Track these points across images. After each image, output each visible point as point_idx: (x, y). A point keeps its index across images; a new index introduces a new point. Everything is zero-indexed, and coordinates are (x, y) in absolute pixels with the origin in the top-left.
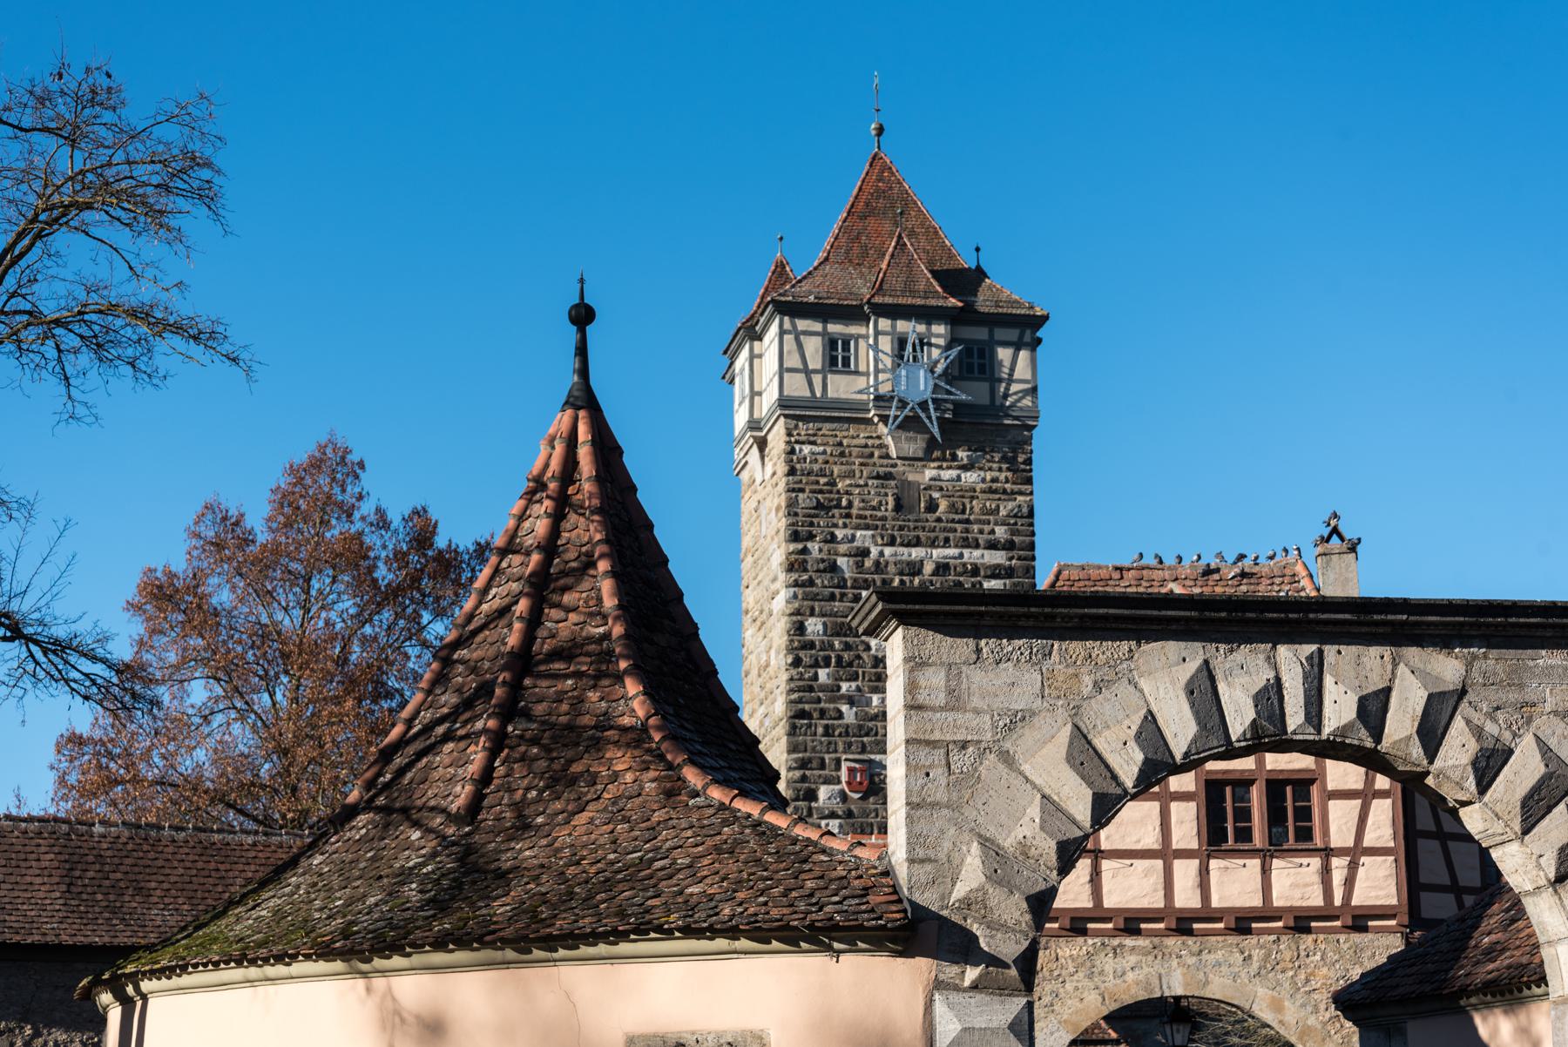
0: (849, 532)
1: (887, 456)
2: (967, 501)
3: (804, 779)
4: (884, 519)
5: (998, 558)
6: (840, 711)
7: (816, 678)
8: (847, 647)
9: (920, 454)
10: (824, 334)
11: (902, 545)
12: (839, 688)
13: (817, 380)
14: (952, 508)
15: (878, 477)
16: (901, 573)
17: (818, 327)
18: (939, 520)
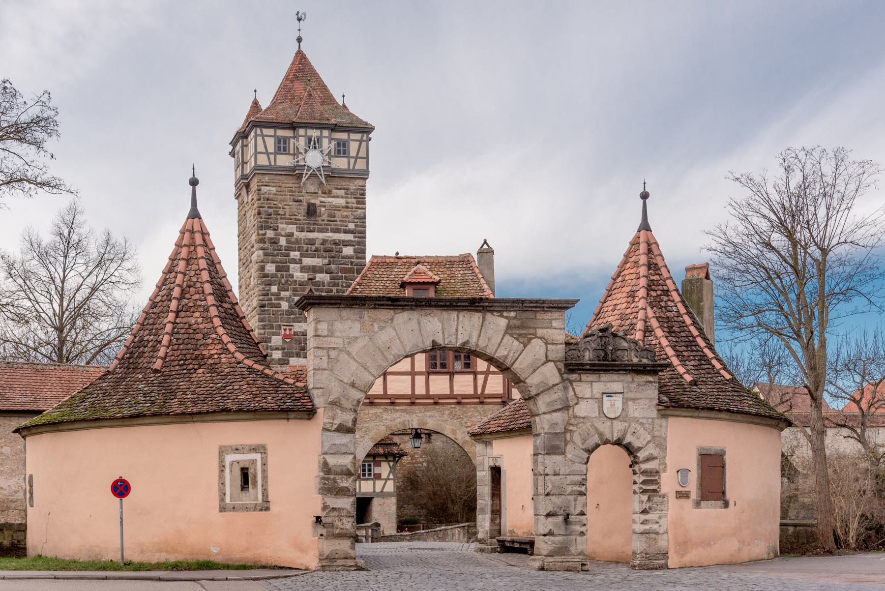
0: (285, 226)
5: (350, 237)
7: (270, 290)
10: (275, 136)
13: (272, 157)
14: (330, 215)
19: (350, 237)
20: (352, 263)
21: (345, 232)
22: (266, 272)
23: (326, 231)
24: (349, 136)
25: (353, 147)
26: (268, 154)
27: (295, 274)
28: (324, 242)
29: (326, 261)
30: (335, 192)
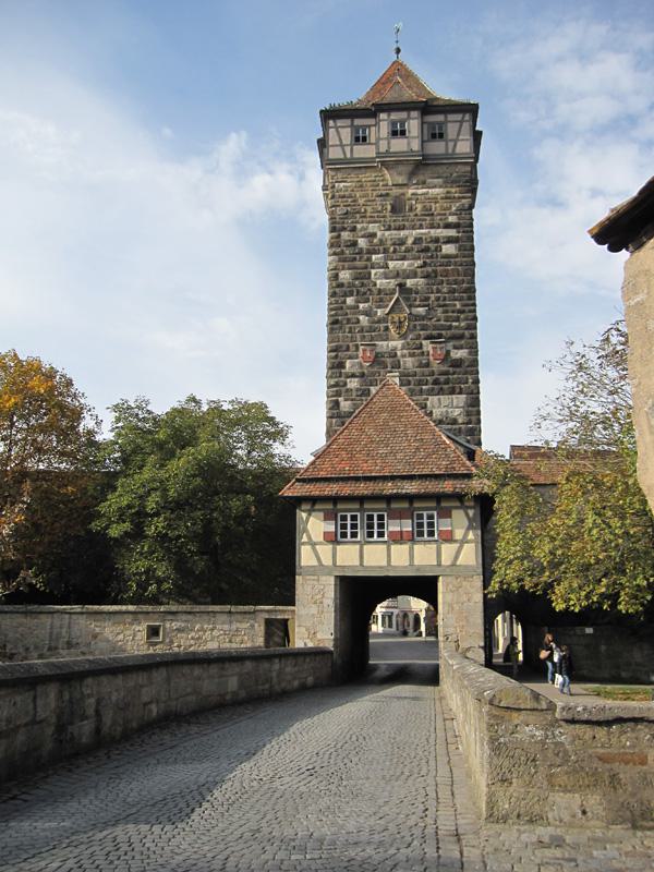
1: (387, 185)
2: (433, 204)
3: (336, 357)
4: (384, 217)
5: (452, 233)
6: (358, 319)
7: (345, 302)
8: (363, 285)
9: (405, 182)
10: (352, 125)
11: (395, 229)
12: (358, 307)
13: (348, 149)
14: (424, 208)
15: (381, 196)
16: (394, 244)
17: (348, 122)
18: (416, 215)
19: (452, 233)
20: (456, 262)
21: (448, 226)
22: (340, 281)
23: (421, 227)
24: (446, 117)
25: (451, 130)
26: (342, 146)
27: (378, 282)
28: (417, 240)
29: (420, 262)
30: (429, 181)
